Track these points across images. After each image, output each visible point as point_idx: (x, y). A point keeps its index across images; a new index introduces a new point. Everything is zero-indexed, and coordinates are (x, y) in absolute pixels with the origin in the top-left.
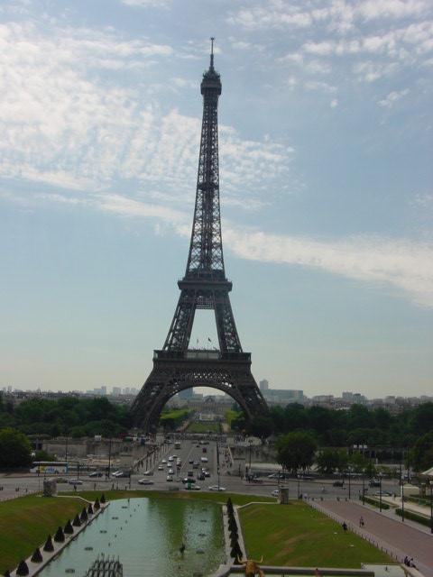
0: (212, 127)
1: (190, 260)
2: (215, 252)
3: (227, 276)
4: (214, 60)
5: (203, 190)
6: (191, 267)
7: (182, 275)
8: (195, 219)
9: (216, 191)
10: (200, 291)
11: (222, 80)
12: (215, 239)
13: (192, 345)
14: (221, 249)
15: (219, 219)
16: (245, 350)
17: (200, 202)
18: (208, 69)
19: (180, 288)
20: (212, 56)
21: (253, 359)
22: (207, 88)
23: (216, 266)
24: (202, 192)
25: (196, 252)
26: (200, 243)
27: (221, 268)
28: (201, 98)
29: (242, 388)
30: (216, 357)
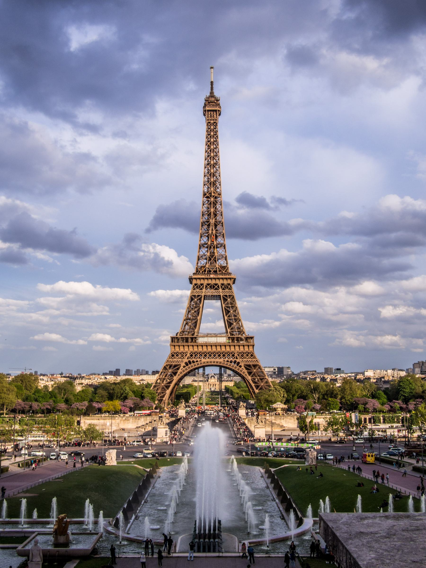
1: (199, 260)
2: (221, 251)
3: (230, 271)
4: (214, 86)
5: (207, 197)
6: (199, 264)
10: (208, 284)
12: (220, 240)
14: (225, 248)
17: (205, 209)
18: (208, 94)
19: (191, 283)
20: (212, 83)
21: (256, 341)
22: (208, 111)
23: (221, 262)
24: (207, 200)
26: (207, 244)
29: (248, 367)
30: (223, 340)
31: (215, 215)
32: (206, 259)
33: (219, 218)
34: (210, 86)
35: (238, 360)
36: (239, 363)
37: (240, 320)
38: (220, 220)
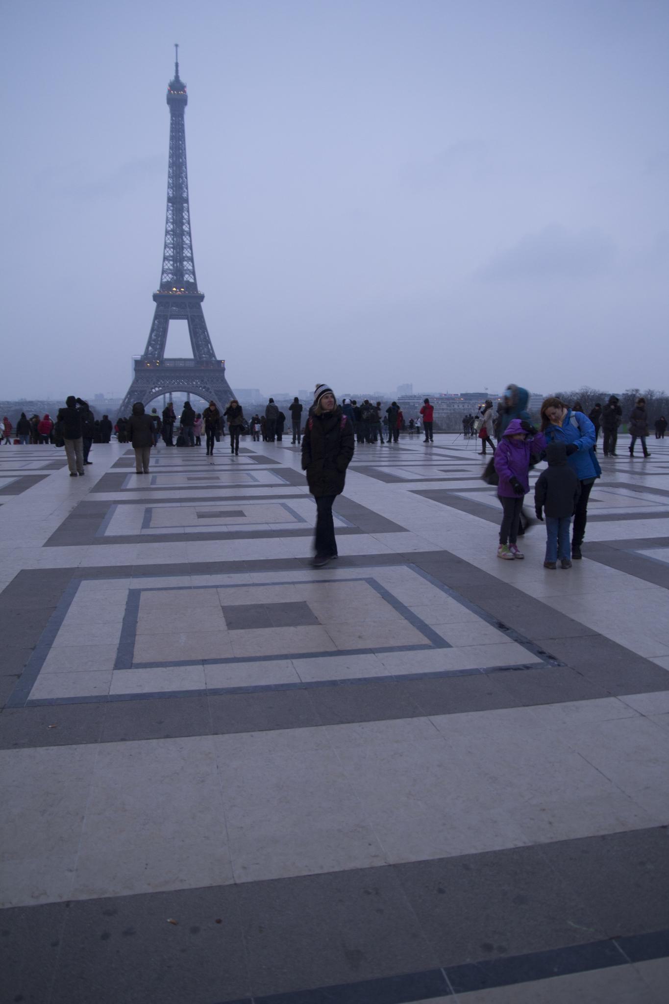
0: (180, 140)
1: (163, 274)
2: (187, 265)
4: (180, 69)
7: (156, 288)
8: (167, 232)
9: (185, 205)
11: (188, 90)
12: (187, 253)
13: (168, 354)
15: (189, 234)
16: (218, 358)
17: (170, 216)
18: (172, 78)
19: (155, 300)
20: (177, 65)
23: (188, 278)
25: (169, 265)
27: (192, 280)
28: (166, 110)
30: (192, 364)
31: (183, 224)
32: (172, 274)
33: (185, 228)
34: (174, 68)
35: (208, 386)
36: (208, 390)
37: (210, 343)
38: (187, 229)
